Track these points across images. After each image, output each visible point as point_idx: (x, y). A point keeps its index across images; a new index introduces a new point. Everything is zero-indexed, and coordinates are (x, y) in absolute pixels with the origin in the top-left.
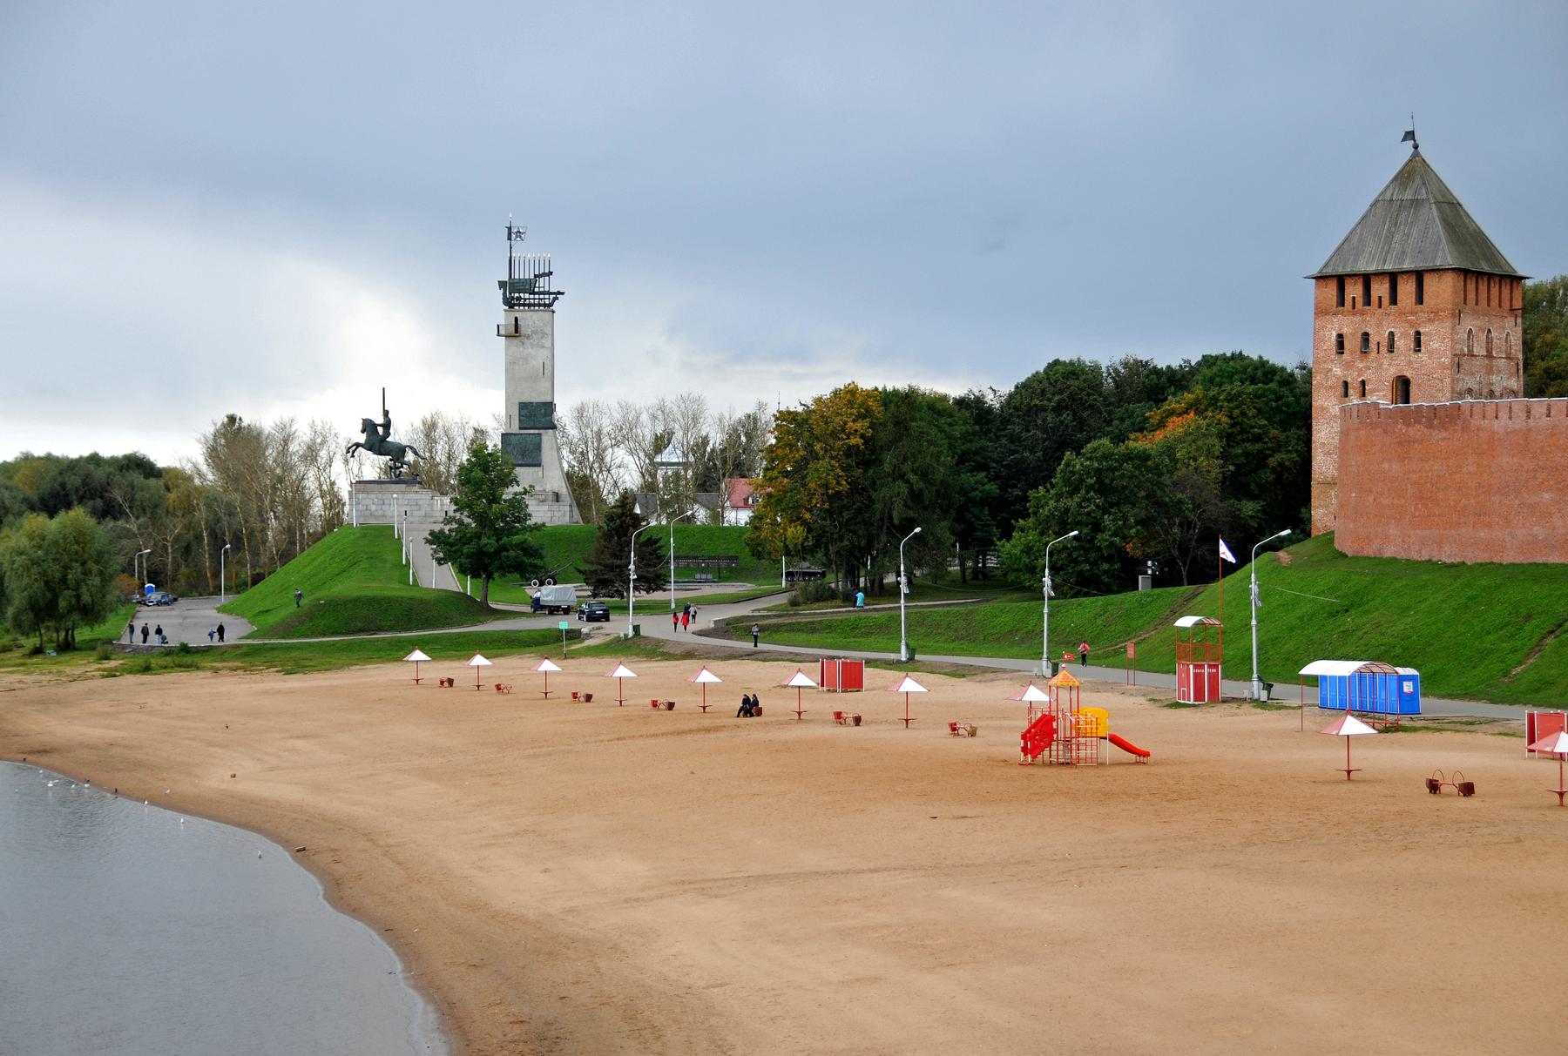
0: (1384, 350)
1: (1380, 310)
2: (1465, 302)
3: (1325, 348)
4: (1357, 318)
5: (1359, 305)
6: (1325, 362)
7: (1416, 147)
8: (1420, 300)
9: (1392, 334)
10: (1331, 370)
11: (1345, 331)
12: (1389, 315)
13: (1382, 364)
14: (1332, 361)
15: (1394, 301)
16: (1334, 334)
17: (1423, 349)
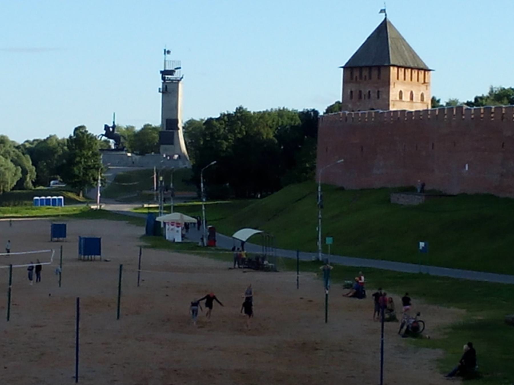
0: (367, 98)
2: (398, 78)
7: (386, 15)
8: (379, 78)
9: (369, 92)
11: (353, 90)
15: (370, 78)
16: (349, 91)
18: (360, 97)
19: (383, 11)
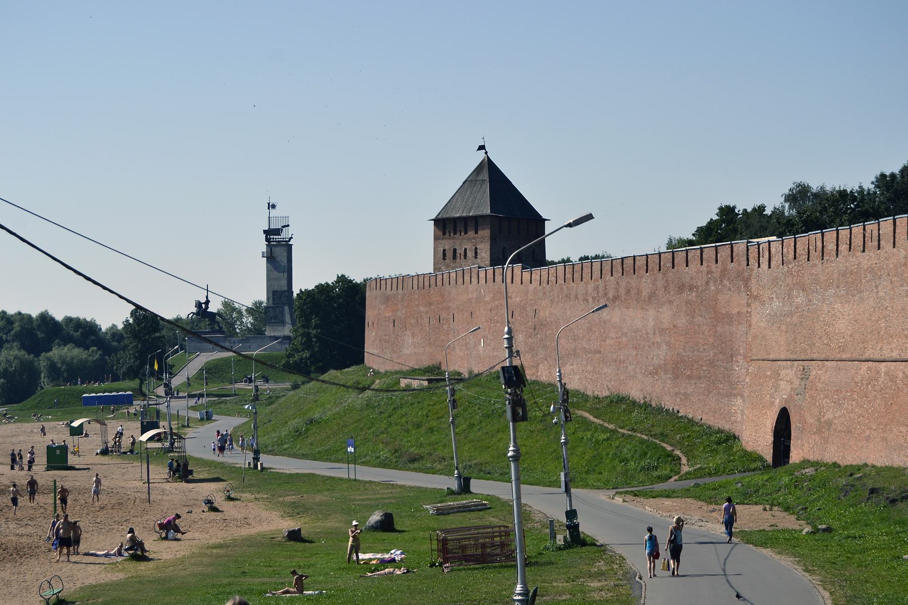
0: (463, 257)
4: (451, 241)
6: (438, 264)
7: (486, 153)
9: (466, 249)
11: (447, 247)
18: (455, 257)
19: (482, 148)
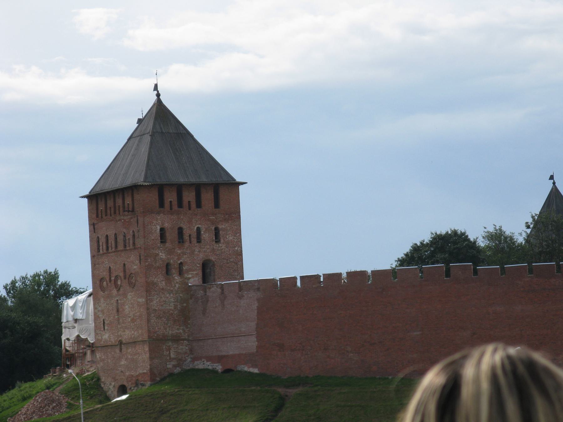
0: (194, 240)
1: (190, 212)
3: (153, 238)
5: (175, 207)
6: (153, 249)
8: (217, 205)
9: (199, 230)
10: (158, 255)
11: (166, 225)
12: (196, 215)
13: (194, 251)
14: (159, 248)
16: (159, 228)
17: (222, 241)
